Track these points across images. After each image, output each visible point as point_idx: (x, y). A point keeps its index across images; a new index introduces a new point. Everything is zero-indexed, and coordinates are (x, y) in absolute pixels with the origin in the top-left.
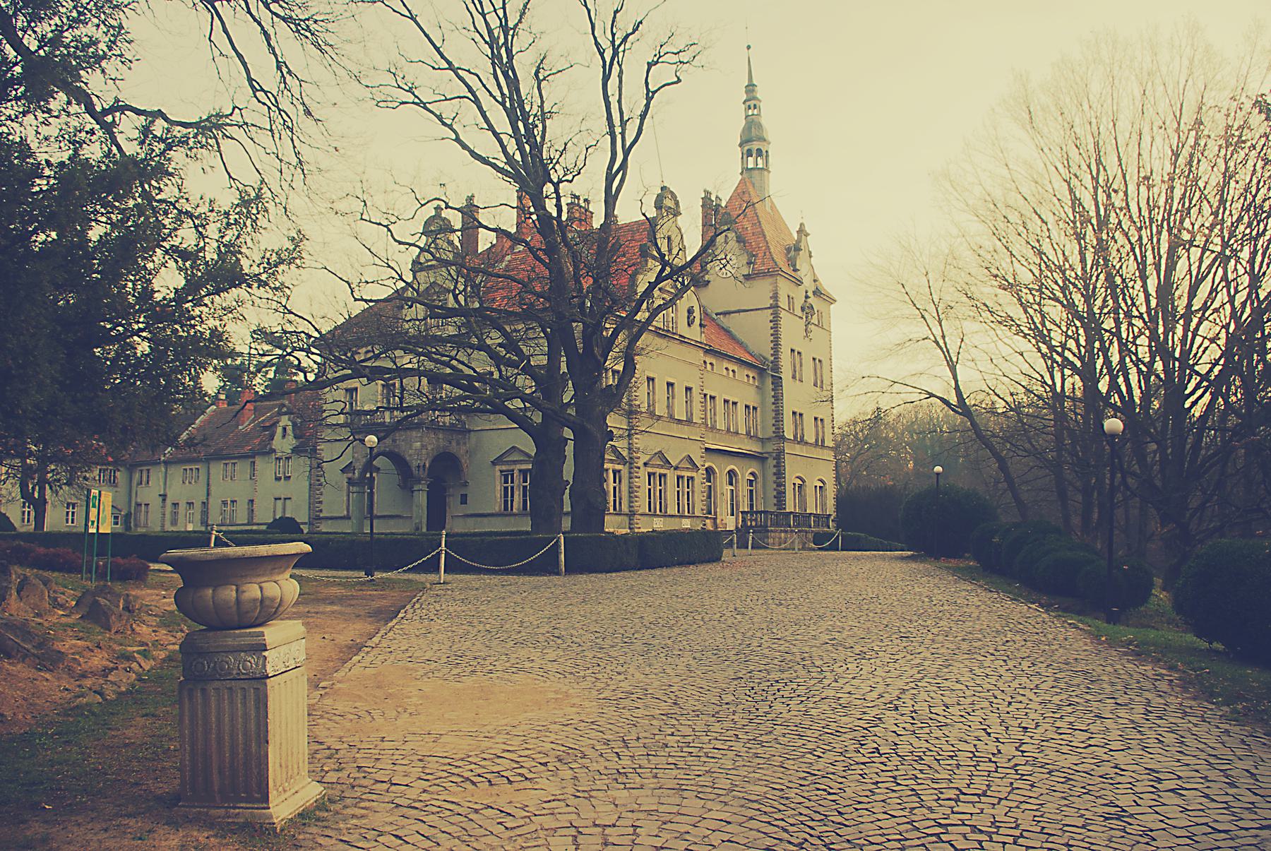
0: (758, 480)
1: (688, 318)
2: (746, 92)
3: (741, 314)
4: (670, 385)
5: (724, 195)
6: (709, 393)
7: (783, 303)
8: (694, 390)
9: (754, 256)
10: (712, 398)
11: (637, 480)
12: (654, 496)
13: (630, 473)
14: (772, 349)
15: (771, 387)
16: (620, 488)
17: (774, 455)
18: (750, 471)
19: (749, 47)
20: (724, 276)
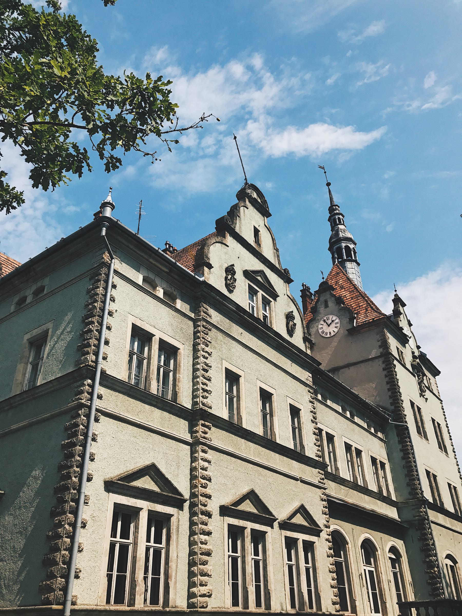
3: (352, 368)
6: (325, 429)
8: (302, 413)
11: (203, 537)
15: (396, 439)
20: (328, 336)
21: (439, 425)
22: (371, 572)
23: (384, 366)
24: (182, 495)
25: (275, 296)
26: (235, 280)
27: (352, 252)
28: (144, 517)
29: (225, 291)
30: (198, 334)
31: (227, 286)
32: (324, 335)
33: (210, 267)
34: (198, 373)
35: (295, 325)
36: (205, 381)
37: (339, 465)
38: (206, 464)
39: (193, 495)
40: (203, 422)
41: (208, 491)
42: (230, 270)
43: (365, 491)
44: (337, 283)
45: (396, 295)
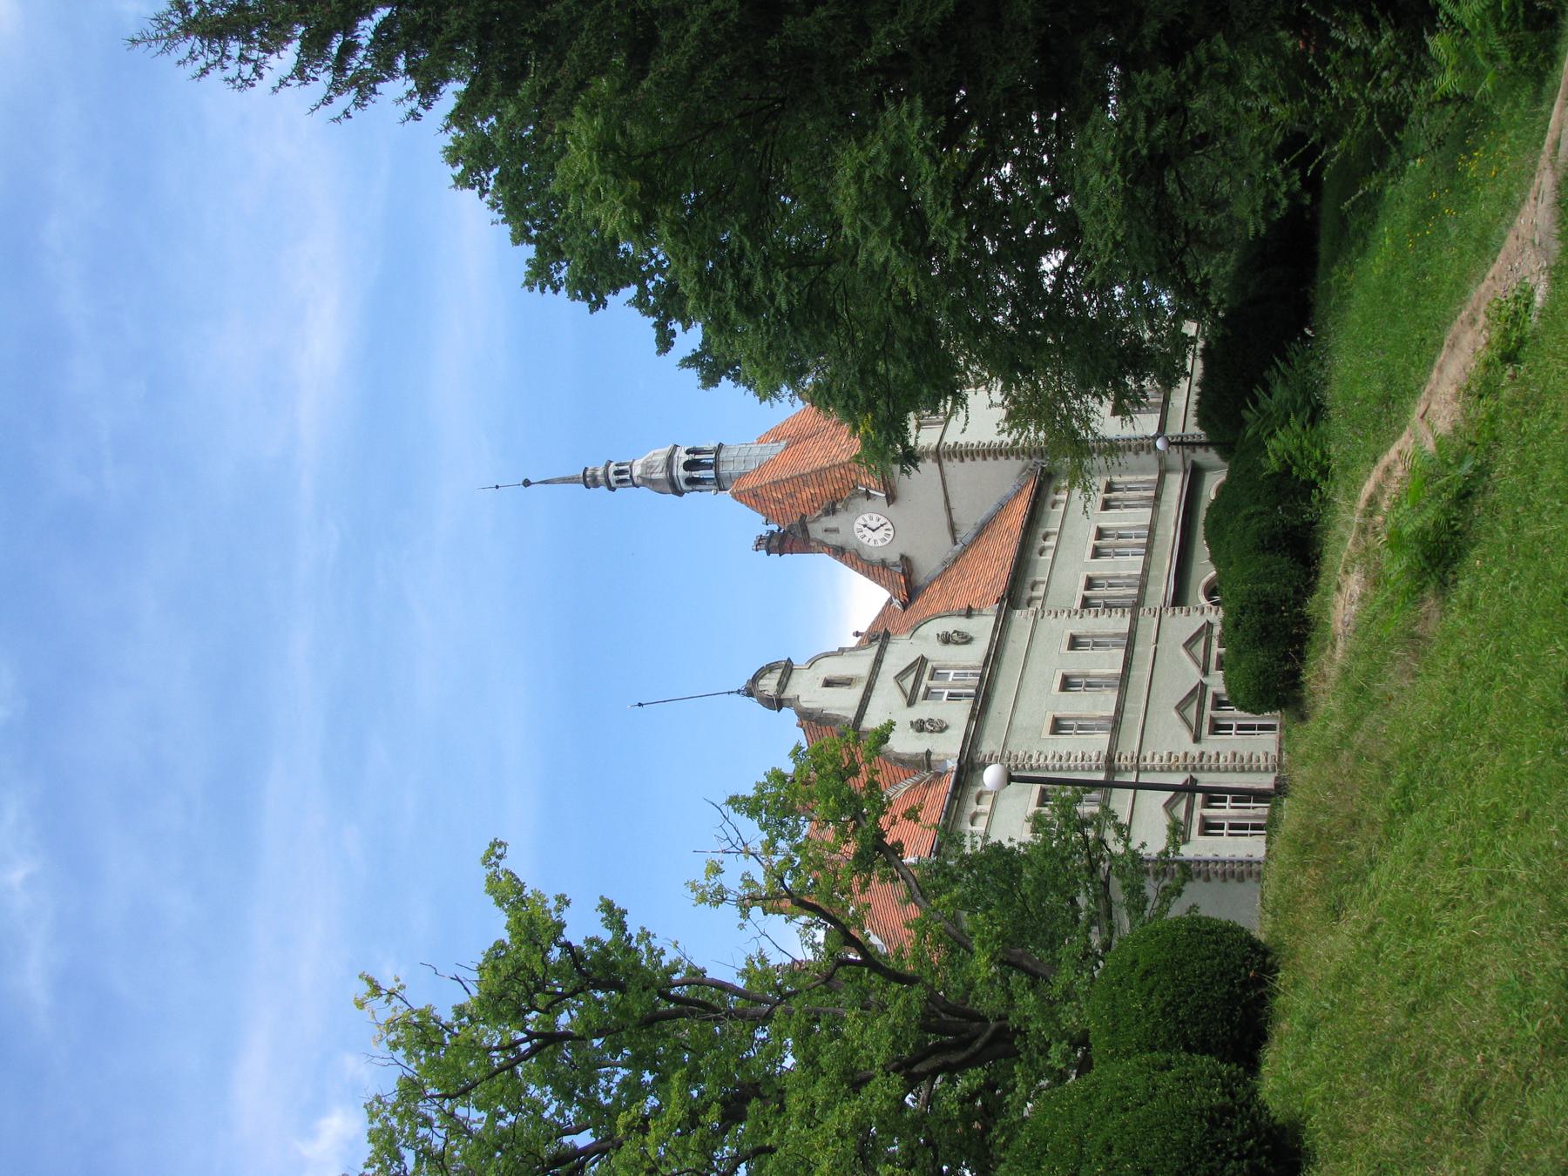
1: (957, 643)
3: (952, 505)
4: (1067, 684)
5: (758, 525)
6: (1080, 591)
8: (1075, 632)
10: (1090, 583)
11: (1222, 759)
13: (1210, 770)
14: (1008, 458)
17: (1187, 452)
19: (527, 483)
20: (891, 533)
23: (956, 461)
25: (922, 661)
28: (1207, 812)
31: (942, 730)
32: (889, 540)
33: (928, 753)
34: (1065, 765)
37: (1124, 573)
38: (1157, 758)
39: (1185, 769)
41: (1181, 755)
42: (920, 726)
43: (1152, 529)
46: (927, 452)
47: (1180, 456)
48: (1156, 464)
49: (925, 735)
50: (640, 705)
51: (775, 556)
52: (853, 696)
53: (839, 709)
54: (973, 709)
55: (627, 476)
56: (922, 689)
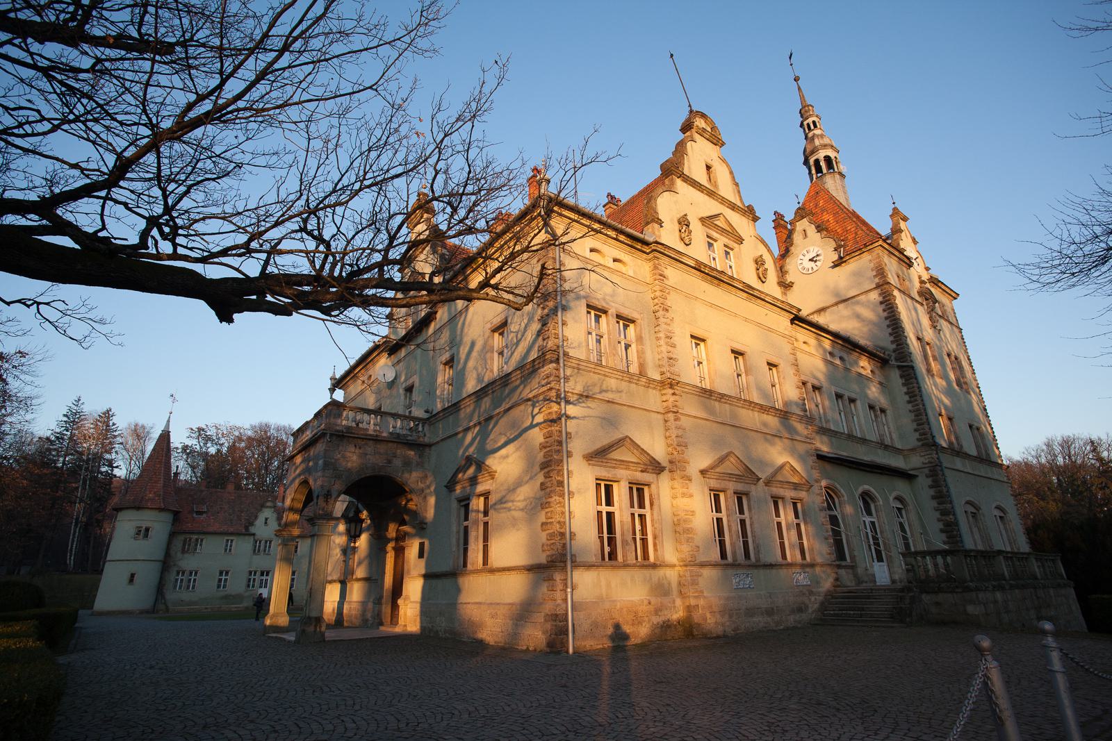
0: (911, 507)
2: (802, 116)
7: (892, 279)
9: (842, 240)
12: (730, 531)
14: (891, 334)
15: (900, 381)
16: (652, 515)
17: (926, 471)
18: (894, 494)
19: (797, 79)
20: (810, 271)
21: (956, 358)
22: (873, 523)
24: (659, 463)
25: (740, 240)
26: (690, 232)
27: (834, 163)
29: (680, 247)
30: (656, 300)
34: (662, 342)
35: (766, 270)
36: (669, 348)
40: (673, 391)
42: (684, 222)
43: (863, 441)
44: (816, 206)
45: (895, 209)
46: (885, 277)
47: (919, 465)
48: (909, 447)
49: (677, 226)
50: (672, 56)
51: (773, 225)
52: (701, 176)
53: (689, 168)
54: (706, 266)
55: (812, 127)
56: (715, 235)
